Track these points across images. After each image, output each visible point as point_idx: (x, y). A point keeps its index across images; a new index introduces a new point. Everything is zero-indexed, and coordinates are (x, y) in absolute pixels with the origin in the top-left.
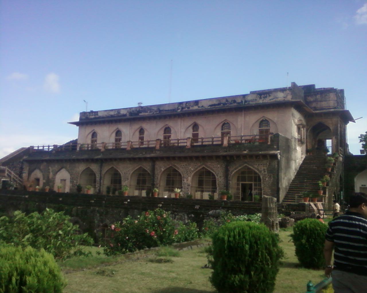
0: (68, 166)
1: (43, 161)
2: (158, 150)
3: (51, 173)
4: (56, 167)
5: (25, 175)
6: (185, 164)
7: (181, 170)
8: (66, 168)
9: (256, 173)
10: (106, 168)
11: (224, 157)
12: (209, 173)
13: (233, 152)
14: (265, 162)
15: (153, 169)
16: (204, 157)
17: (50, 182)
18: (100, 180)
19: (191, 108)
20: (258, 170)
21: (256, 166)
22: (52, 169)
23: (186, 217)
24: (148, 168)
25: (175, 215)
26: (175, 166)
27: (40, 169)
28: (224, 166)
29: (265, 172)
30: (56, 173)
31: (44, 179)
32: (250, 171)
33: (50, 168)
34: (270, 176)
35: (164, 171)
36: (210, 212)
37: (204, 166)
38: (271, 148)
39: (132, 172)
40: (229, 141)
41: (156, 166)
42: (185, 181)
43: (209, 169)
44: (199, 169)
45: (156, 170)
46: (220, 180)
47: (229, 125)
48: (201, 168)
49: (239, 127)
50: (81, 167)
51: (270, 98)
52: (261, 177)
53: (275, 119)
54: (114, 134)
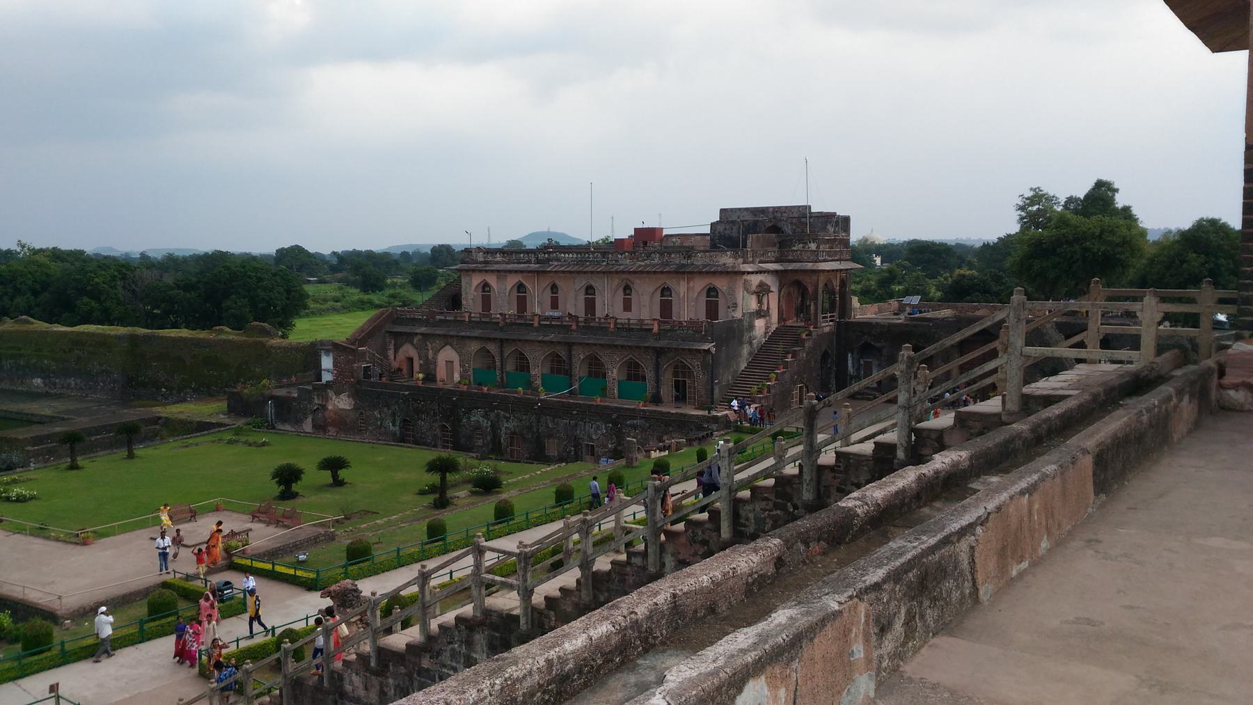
1: (417, 334)
3: (431, 351)
5: (391, 353)
7: (604, 359)
10: (508, 350)
12: (637, 366)
13: (663, 343)
15: (570, 357)
18: (502, 365)
20: (691, 364)
21: (689, 360)
23: (604, 427)
24: (564, 353)
25: (592, 424)
26: (597, 353)
27: (412, 344)
29: (699, 368)
30: (437, 352)
31: (420, 358)
32: (685, 366)
33: (428, 343)
34: (704, 373)
35: (583, 359)
37: (631, 356)
39: (542, 358)
41: (574, 352)
42: (610, 374)
43: (637, 360)
44: (625, 360)
45: (573, 358)
46: (650, 375)
47: (671, 291)
48: (628, 358)
49: (682, 295)
50: (474, 347)
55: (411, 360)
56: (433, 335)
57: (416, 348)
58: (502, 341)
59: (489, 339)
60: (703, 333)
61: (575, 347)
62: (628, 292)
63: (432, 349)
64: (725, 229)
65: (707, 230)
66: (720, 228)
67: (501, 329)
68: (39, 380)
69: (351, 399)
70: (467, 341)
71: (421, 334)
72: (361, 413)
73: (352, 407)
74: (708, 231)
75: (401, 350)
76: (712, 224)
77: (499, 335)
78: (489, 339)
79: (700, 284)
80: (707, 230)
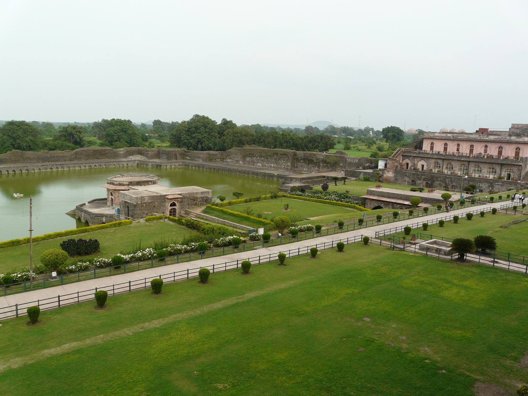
0: (426, 159)
2: (471, 158)
4: (419, 159)
6: (483, 164)
8: (424, 160)
9: (512, 170)
11: (501, 164)
13: (504, 162)
14: (517, 167)
16: (492, 163)
17: (414, 165)
19: (485, 139)
22: (416, 160)
28: (500, 166)
31: (412, 163)
36: (496, 184)
38: (520, 162)
40: (503, 157)
51: (522, 139)
52: (515, 172)
53: (523, 148)
54: (444, 145)
55: (408, 164)
56: (418, 157)
57: (410, 160)
58: (444, 159)
59: (439, 159)
60: (519, 160)
61: (471, 163)
62: (486, 147)
63: (417, 161)
64: (515, 130)
65: (508, 130)
66: (512, 130)
67: (444, 156)
68: (260, 164)
69: (393, 174)
70: (430, 159)
71: (413, 156)
72: (397, 178)
73: (393, 176)
74: (508, 131)
75: (404, 161)
76: (510, 128)
77: (443, 158)
78: (439, 159)
79: (514, 147)
80: (508, 130)
